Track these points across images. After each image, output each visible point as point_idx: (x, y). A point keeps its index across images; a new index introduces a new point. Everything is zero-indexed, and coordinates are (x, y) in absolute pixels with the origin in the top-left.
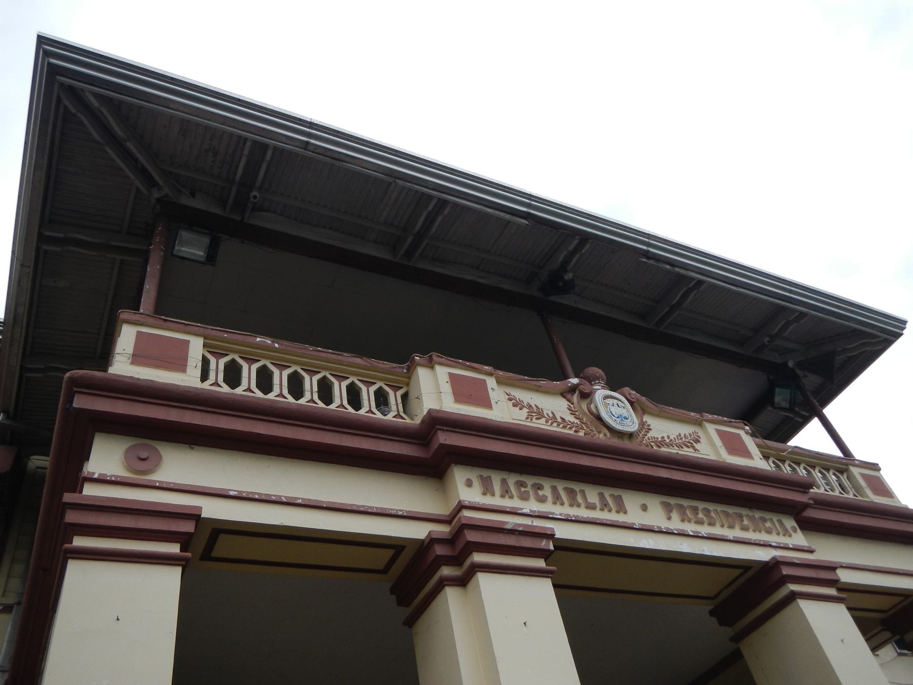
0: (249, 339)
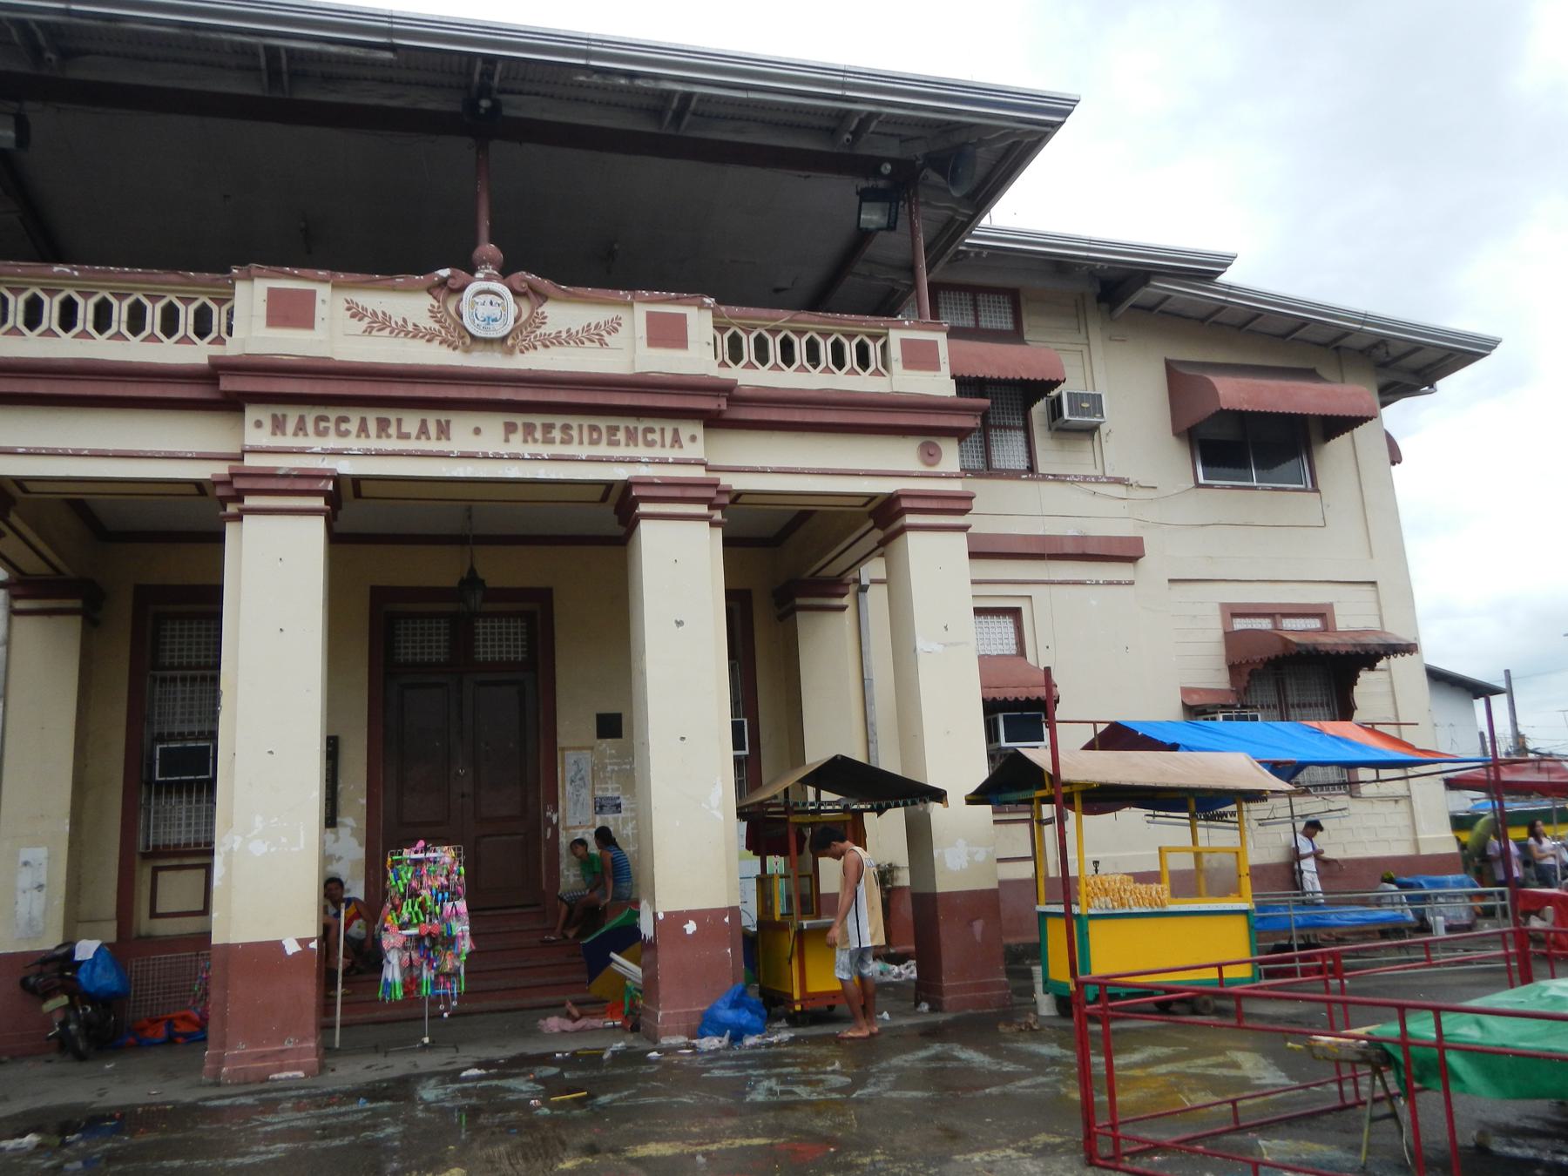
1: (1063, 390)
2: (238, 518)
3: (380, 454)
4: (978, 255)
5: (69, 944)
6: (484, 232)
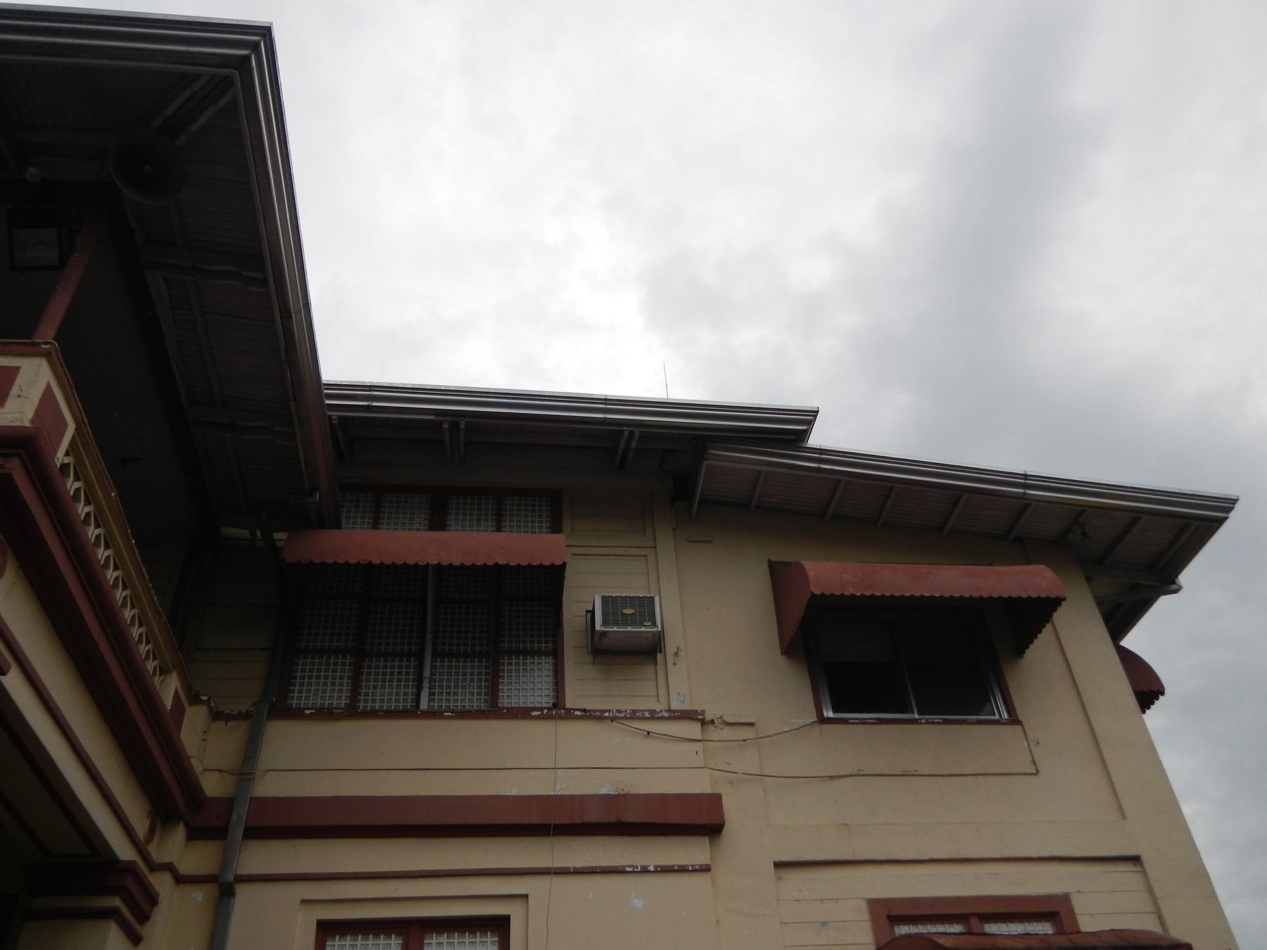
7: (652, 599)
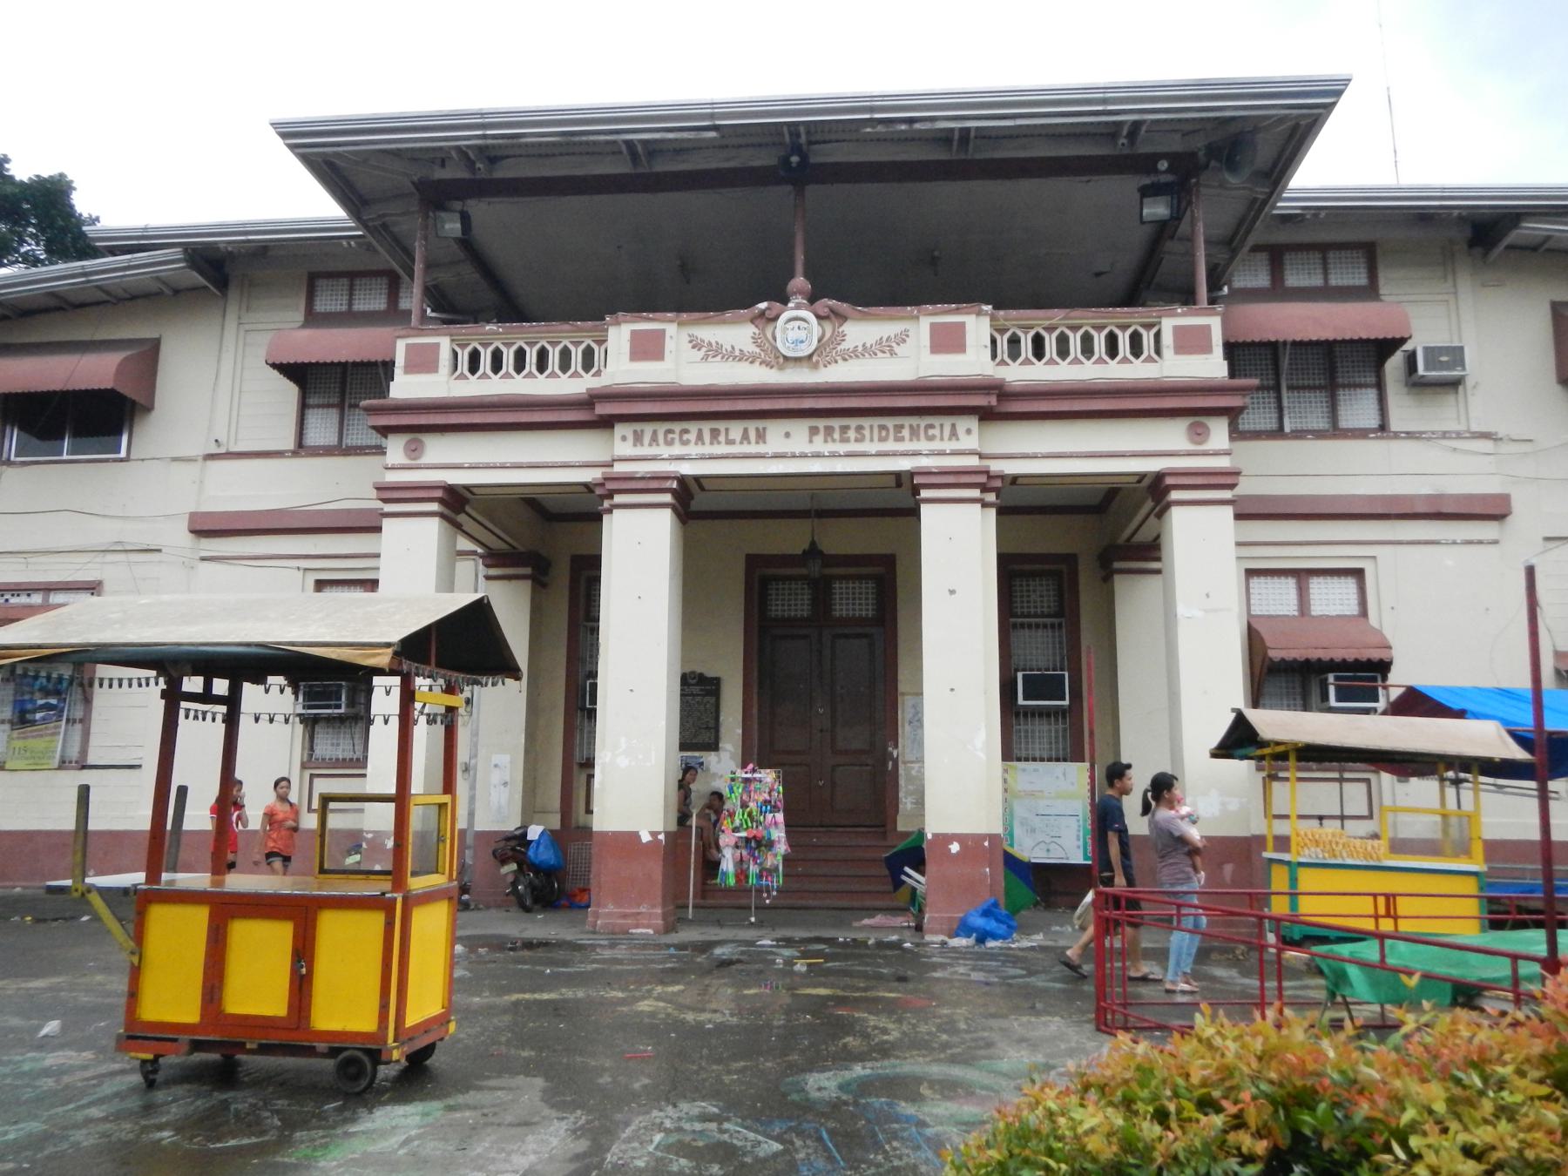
0: (480, 330)
1: (1417, 343)
2: (610, 511)
3: (712, 458)
4: (1315, 215)
5: (524, 827)
6: (799, 267)
7: (1461, 349)
